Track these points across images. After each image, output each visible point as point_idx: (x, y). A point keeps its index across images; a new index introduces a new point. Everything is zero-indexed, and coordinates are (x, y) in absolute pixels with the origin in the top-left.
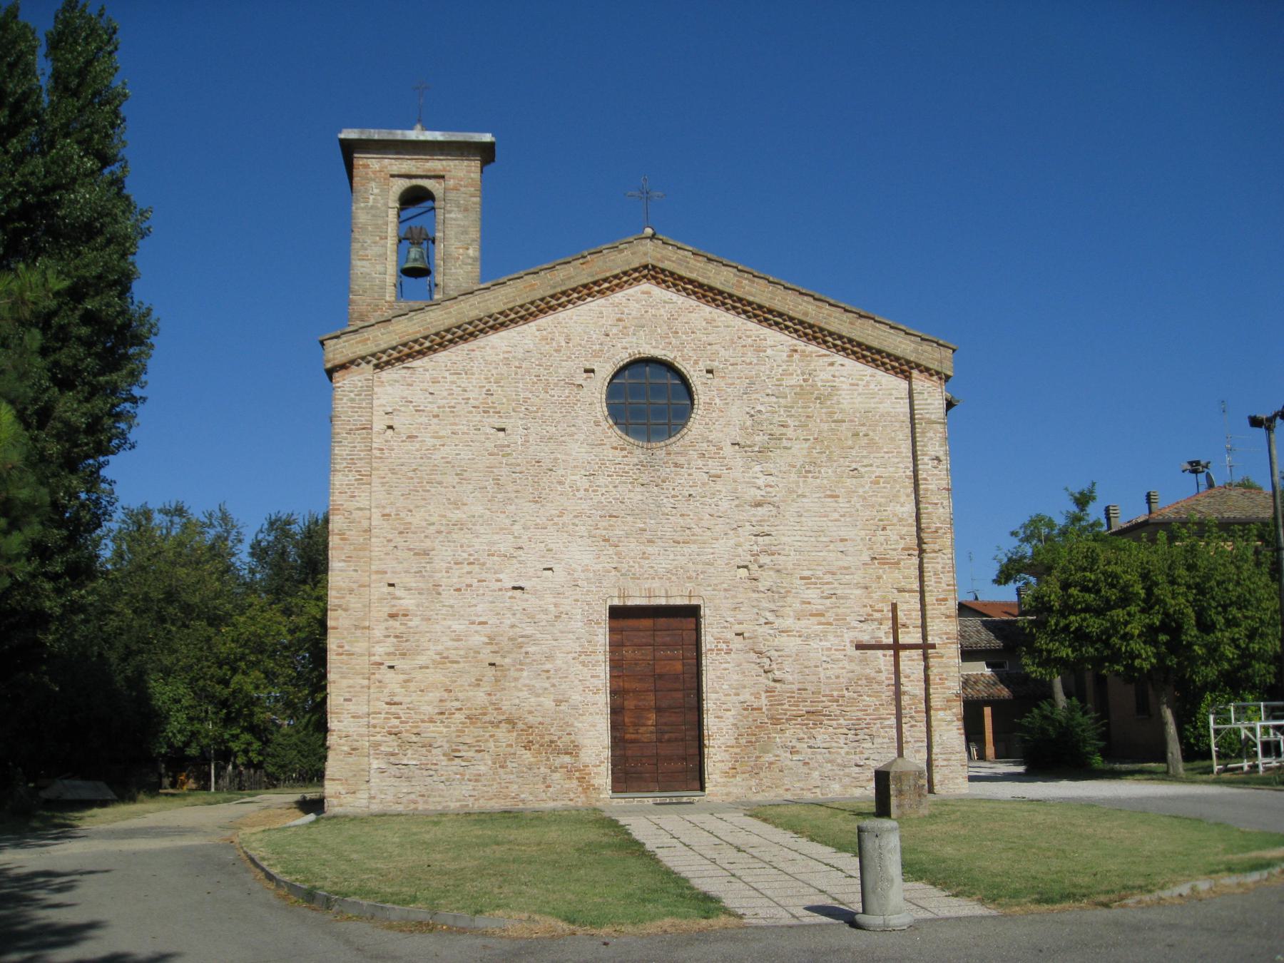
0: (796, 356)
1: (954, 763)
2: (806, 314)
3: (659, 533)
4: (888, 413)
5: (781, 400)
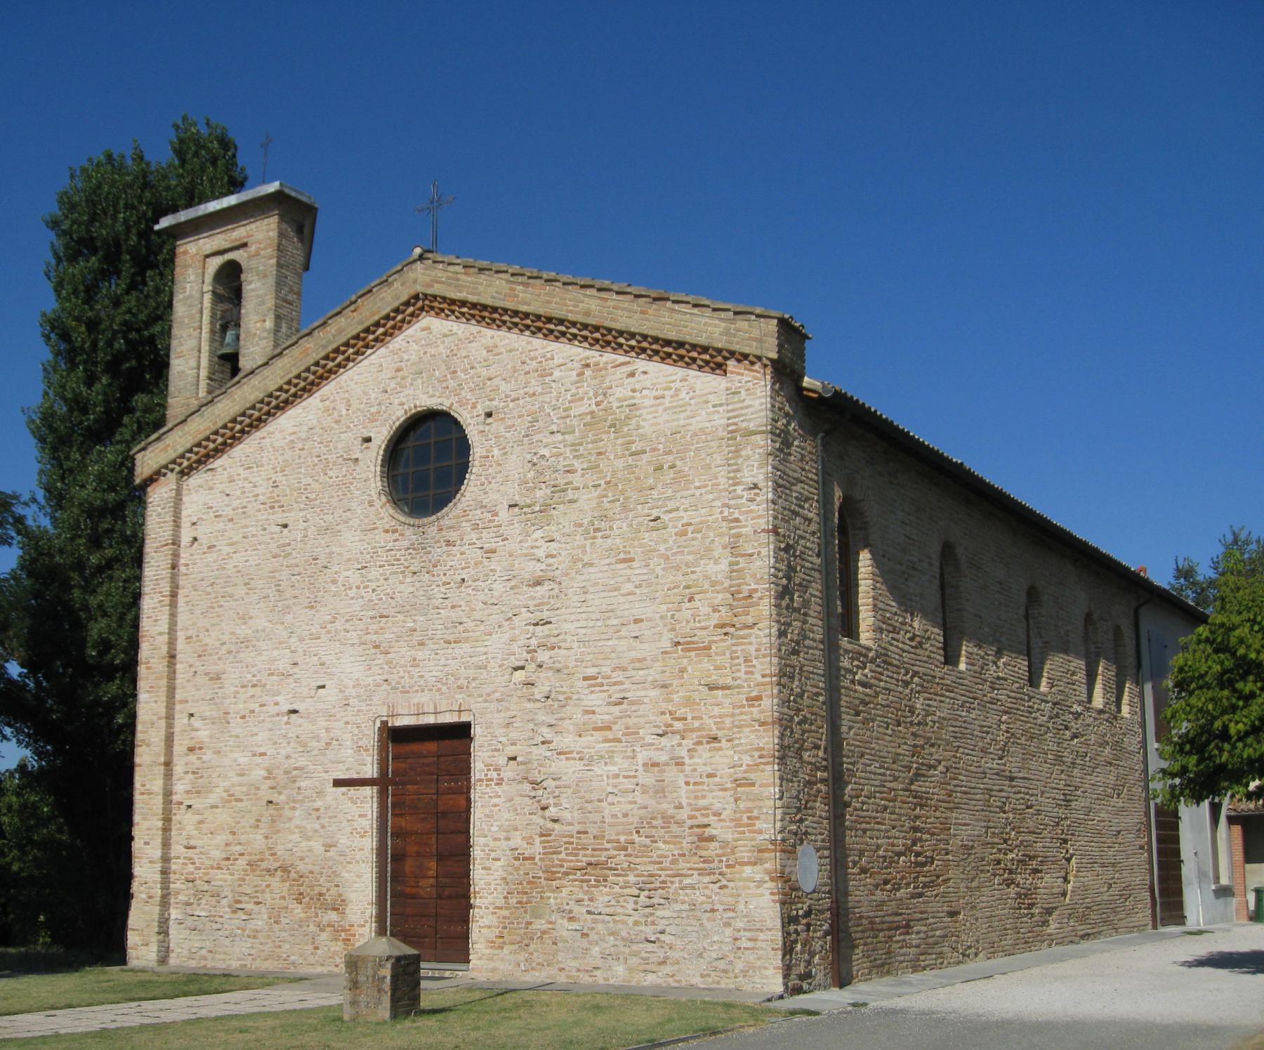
0: (588, 372)
1: (763, 945)
2: (587, 314)
3: (430, 633)
4: (702, 430)
5: (567, 437)
